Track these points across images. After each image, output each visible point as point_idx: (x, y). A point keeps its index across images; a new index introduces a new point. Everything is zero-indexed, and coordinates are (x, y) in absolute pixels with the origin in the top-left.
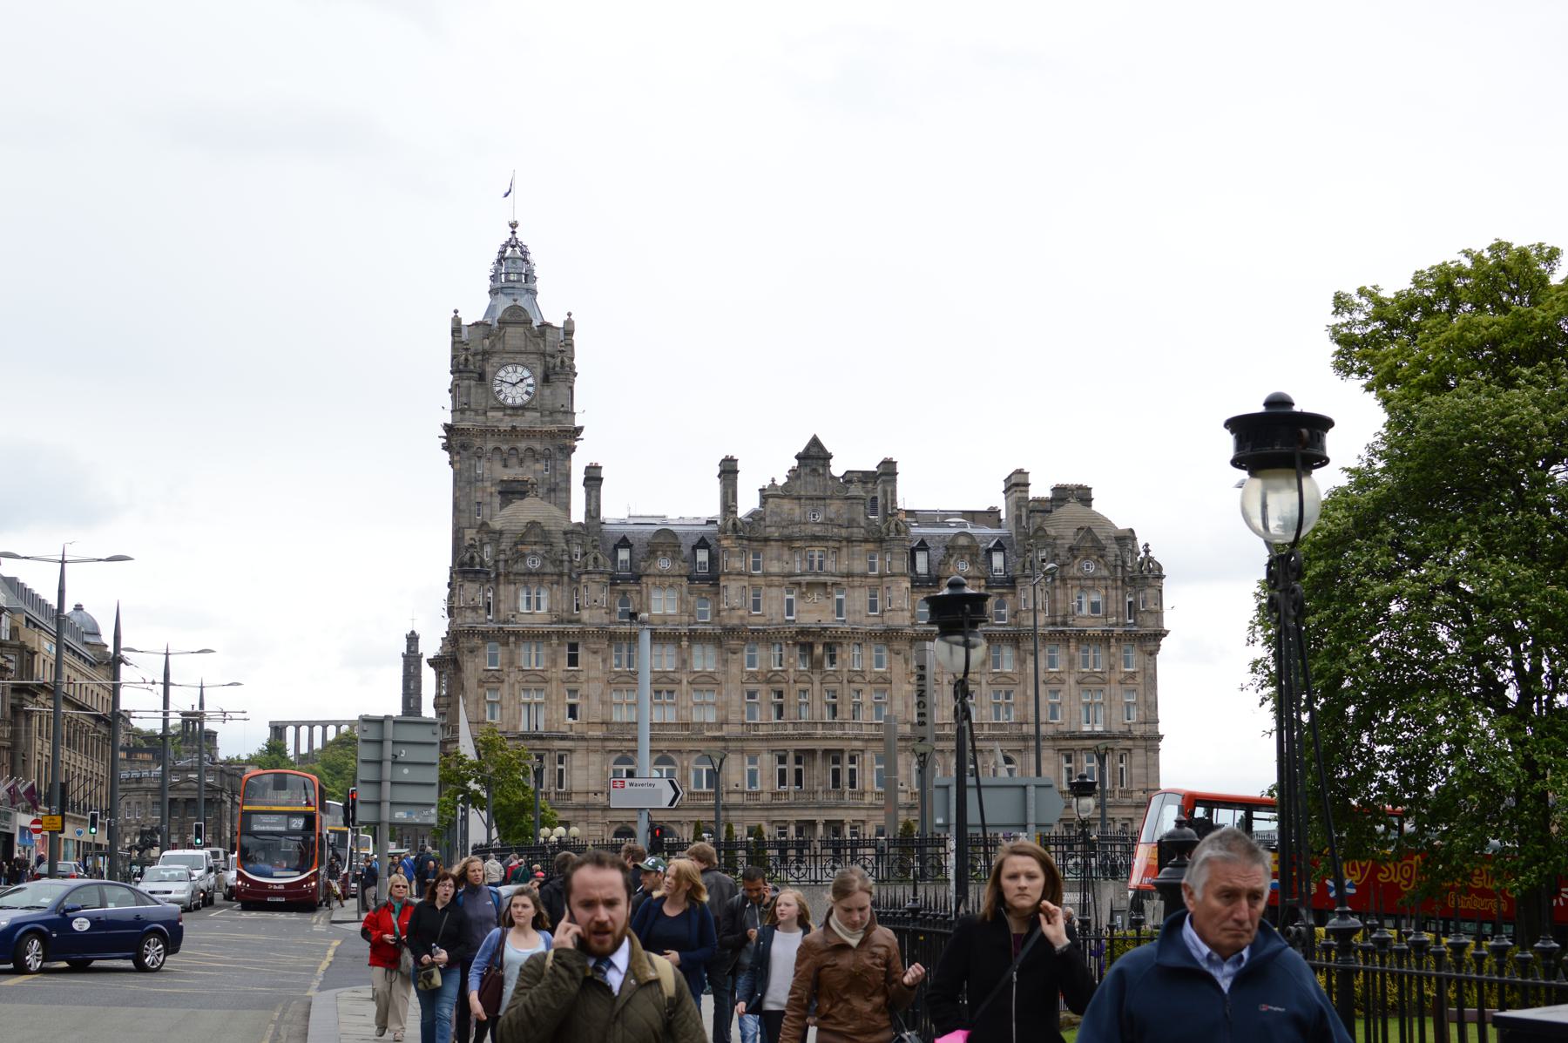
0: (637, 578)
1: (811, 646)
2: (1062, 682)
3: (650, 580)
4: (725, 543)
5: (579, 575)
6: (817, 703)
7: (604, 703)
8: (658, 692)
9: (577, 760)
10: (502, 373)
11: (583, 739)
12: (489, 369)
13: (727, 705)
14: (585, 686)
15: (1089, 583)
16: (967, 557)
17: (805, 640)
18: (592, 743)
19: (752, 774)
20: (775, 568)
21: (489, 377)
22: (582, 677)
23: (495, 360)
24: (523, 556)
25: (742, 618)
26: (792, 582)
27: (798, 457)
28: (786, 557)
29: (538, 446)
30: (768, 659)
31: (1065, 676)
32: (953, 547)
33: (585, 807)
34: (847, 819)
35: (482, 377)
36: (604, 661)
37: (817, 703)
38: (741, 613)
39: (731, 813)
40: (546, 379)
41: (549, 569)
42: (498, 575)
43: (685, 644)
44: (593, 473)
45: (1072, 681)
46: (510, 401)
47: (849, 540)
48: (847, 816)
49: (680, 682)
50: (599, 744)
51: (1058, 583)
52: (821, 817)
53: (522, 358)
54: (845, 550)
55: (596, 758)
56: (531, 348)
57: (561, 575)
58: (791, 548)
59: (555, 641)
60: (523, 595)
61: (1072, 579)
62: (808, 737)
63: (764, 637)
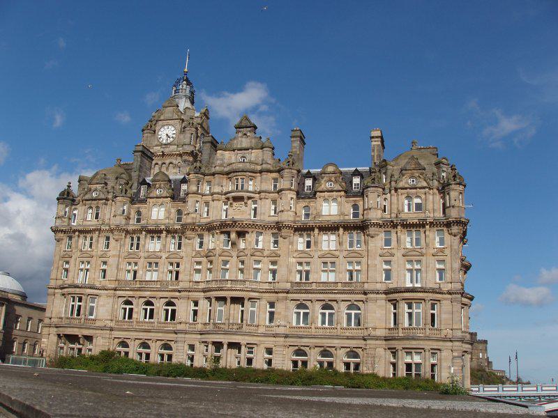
1: (228, 234)
2: (392, 255)
8: (150, 263)
10: (162, 130)
16: (333, 179)
19: (195, 312)
20: (217, 189)
29: (174, 162)
31: (394, 251)
35: (155, 131)
37: (235, 269)
38: (194, 215)
40: (183, 130)
45: (399, 254)
46: (164, 142)
48: (242, 340)
50: (113, 292)
51: (393, 192)
52: (225, 339)
54: (259, 178)
56: (177, 117)
57: (107, 200)
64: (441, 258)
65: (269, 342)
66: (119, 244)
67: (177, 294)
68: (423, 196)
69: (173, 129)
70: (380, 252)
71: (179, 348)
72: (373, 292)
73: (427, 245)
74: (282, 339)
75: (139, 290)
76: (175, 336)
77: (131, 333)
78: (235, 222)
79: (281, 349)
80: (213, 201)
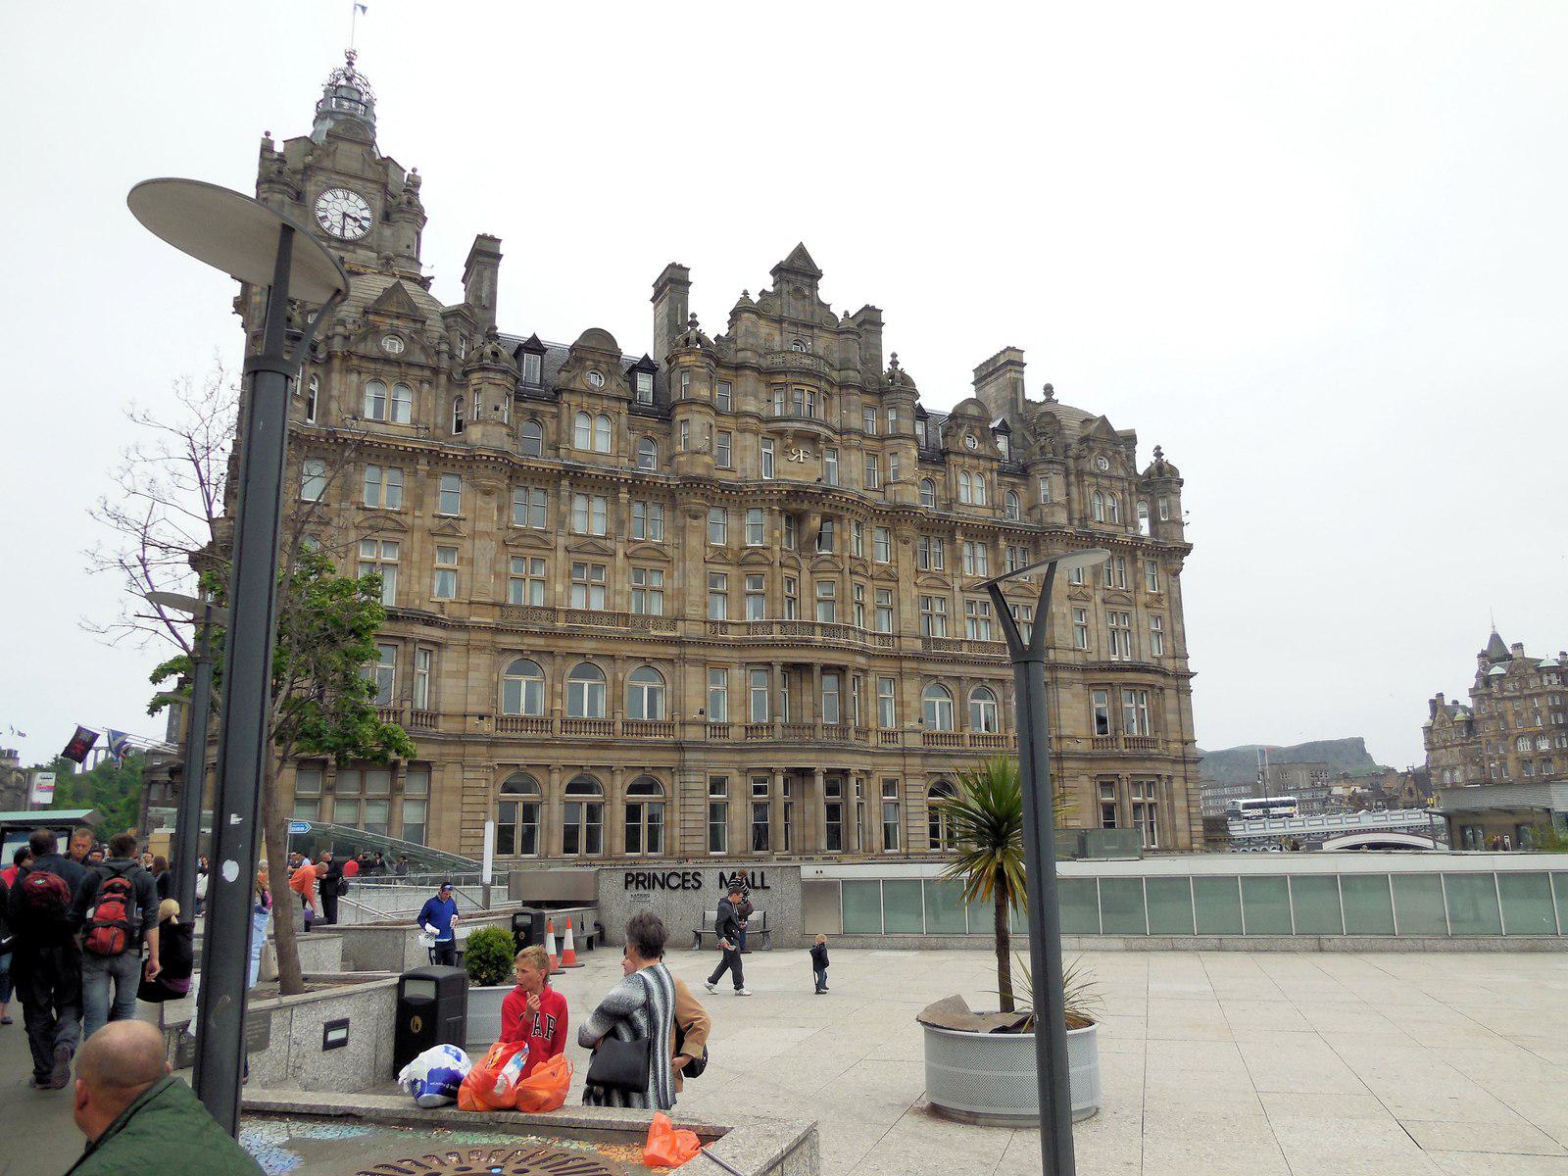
0: (555, 395)
2: (1087, 598)
3: (575, 400)
4: (685, 360)
5: (466, 374)
6: (806, 601)
7: (497, 575)
9: (450, 661)
10: (328, 196)
11: (461, 626)
12: (310, 188)
13: (681, 594)
14: (467, 544)
15: (1106, 482)
16: (977, 432)
17: (799, 509)
18: (475, 636)
21: (310, 198)
22: (465, 529)
23: (322, 177)
24: (375, 332)
25: (708, 466)
26: (775, 432)
27: (774, 272)
28: (763, 396)
30: (741, 532)
31: (1090, 591)
32: (963, 416)
33: (461, 740)
34: (854, 768)
35: (299, 197)
36: (500, 509)
39: (689, 756)
40: (387, 217)
41: (419, 357)
42: (330, 357)
43: (624, 496)
44: (487, 246)
45: (1098, 599)
46: (337, 232)
47: (844, 386)
49: (613, 555)
50: (487, 636)
51: (1072, 478)
52: (820, 763)
53: (358, 184)
54: (836, 400)
55: (481, 660)
56: (370, 175)
57: (436, 371)
58: (770, 385)
59: (423, 466)
60: (370, 392)
61: (1092, 474)
62: (807, 645)
63: (733, 497)
64: (1157, 612)
65: (891, 768)
66: (494, 505)
67: (673, 651)
68: (1120, 496)
69: (362, 204)
70: (1067, 590)
71: (693, 786)
72: (1068, 667)
73: (1137, 587)
74: (917, 761)
75: (569, 635)
76: (675, 756)
77: (553, 752)
78: (827, 491)
79: (916, 782)
80: (743, 431)
